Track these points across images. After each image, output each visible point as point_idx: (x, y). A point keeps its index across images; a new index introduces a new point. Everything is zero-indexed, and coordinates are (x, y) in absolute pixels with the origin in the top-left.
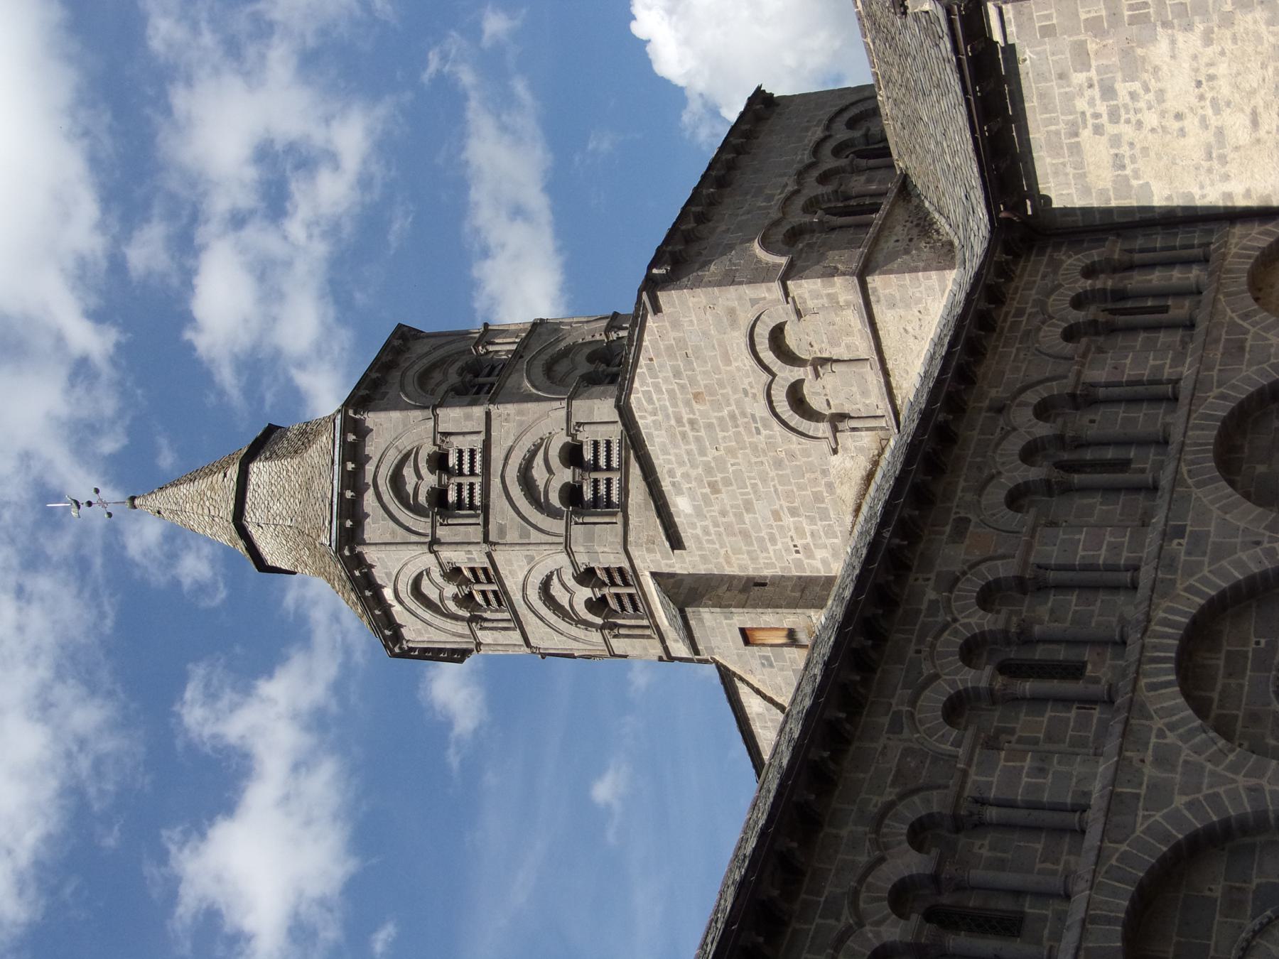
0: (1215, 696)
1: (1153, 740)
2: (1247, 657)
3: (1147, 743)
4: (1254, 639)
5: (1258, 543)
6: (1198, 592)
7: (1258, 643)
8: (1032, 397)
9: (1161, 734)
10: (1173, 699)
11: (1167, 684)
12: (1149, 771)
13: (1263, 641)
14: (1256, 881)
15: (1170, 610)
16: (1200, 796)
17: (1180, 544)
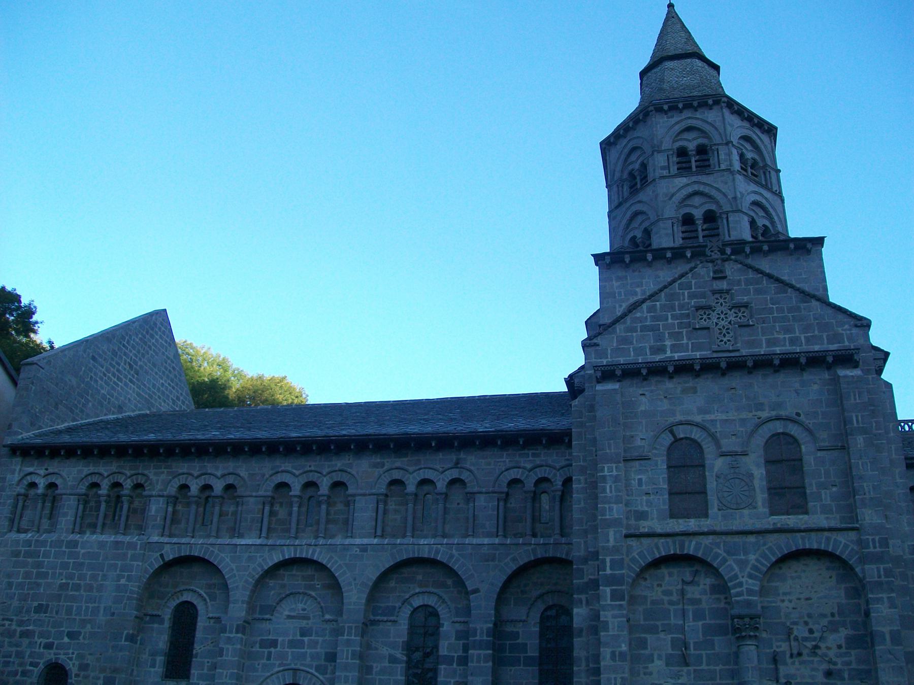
0: (294, 572)
1: (259, 555)
2: (312, 581)
3: (257, 553)
4: (320, 583)
5: (355, 580)
6: (329, 561)
7: (318, 585)
8: (465, 476)
9: (261, 557)
10: (277, 558)
11: (283, 555)
12: (246, 555)
13: (319, 586)
14: (217, 592)
15: (320, 553)
16: (235, 572)
17: (356, 551)
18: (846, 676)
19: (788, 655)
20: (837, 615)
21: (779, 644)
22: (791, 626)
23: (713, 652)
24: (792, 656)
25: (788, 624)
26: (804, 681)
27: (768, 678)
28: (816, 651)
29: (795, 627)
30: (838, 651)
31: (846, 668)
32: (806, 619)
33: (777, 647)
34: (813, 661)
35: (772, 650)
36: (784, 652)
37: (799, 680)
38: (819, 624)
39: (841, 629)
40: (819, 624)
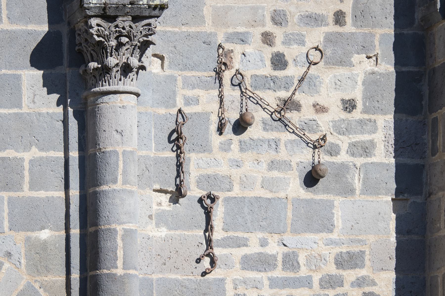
18: (358, 185)
19: (214, 127)
20: (349, 19)
21: (190, 93)
22: (228, 46)
23: (15, 110)
24: (220, 130)
25: (220, 39)
26: (250, 194)
27: (158, 187)
28: (288, 115)
29: (238, 49)
30: (344, 115)
31: (360, 161)
32: (270, 27)
33: (188, 101)
34: (277, 143)
35: (174, 111)
36: (205, 116)
37: (236, 192)
38: (302, 43)
39: (356, 58)
40: (302, 43)
